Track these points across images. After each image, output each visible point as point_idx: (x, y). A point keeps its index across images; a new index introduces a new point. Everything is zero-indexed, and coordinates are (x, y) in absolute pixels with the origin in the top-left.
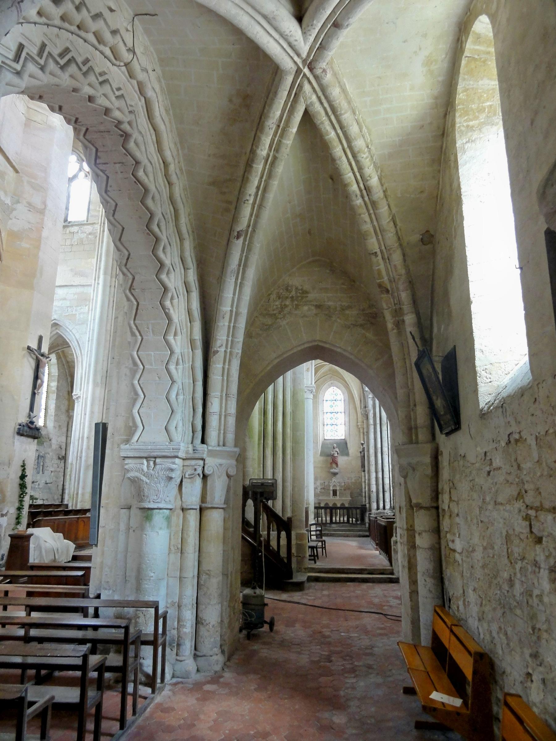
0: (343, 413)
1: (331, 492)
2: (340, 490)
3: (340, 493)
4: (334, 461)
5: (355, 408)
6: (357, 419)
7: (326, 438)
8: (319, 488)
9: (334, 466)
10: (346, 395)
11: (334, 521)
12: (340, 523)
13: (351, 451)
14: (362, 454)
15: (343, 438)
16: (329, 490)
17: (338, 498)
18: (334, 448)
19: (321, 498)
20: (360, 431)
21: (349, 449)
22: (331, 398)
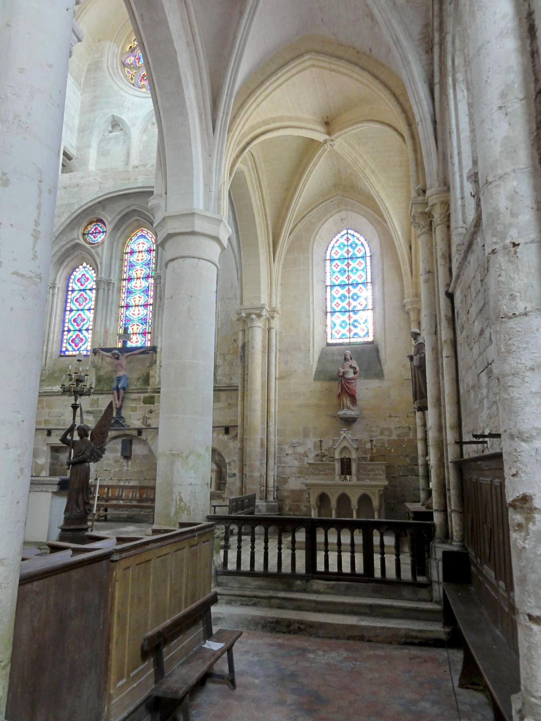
0: (369, 286)
1: (338, 466)
2: (360, 459)
3: (358, 471)
4: (346, 391)
5: (398, 268)
6: (403, 292)
7: (330, 341)
8: (312, 455)
9: (347, 401)
10: (376, 242)
11: (321, 567)
12: (339, 576)
13: (386, 368)
14: (416, 362)
15: (370, 339)
16: (332, 459)
17: (352, 480)
18: (346, 359)
19: (311, 480)
20: (409, 318)
21: (383, 362)
22: (342, 253)
